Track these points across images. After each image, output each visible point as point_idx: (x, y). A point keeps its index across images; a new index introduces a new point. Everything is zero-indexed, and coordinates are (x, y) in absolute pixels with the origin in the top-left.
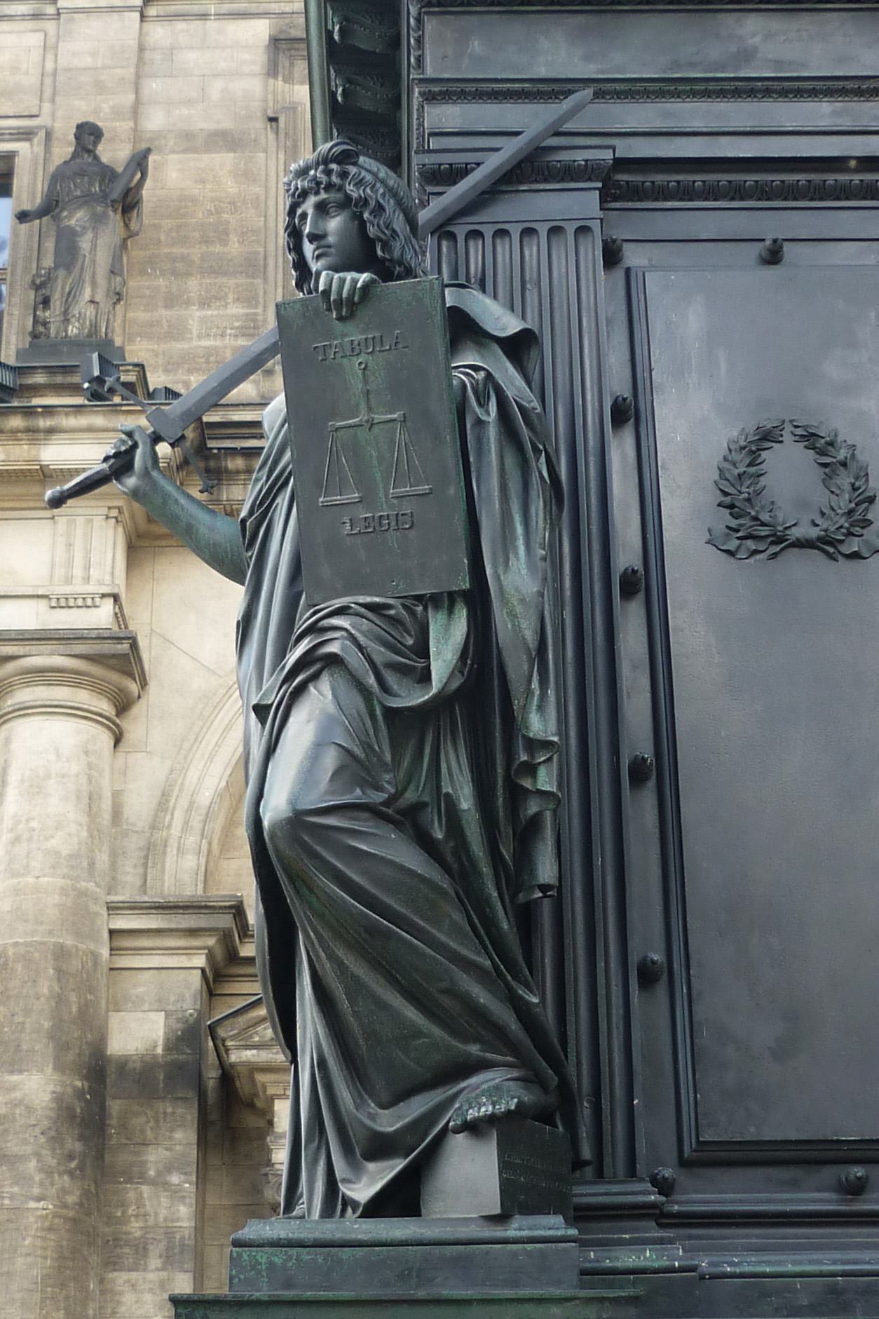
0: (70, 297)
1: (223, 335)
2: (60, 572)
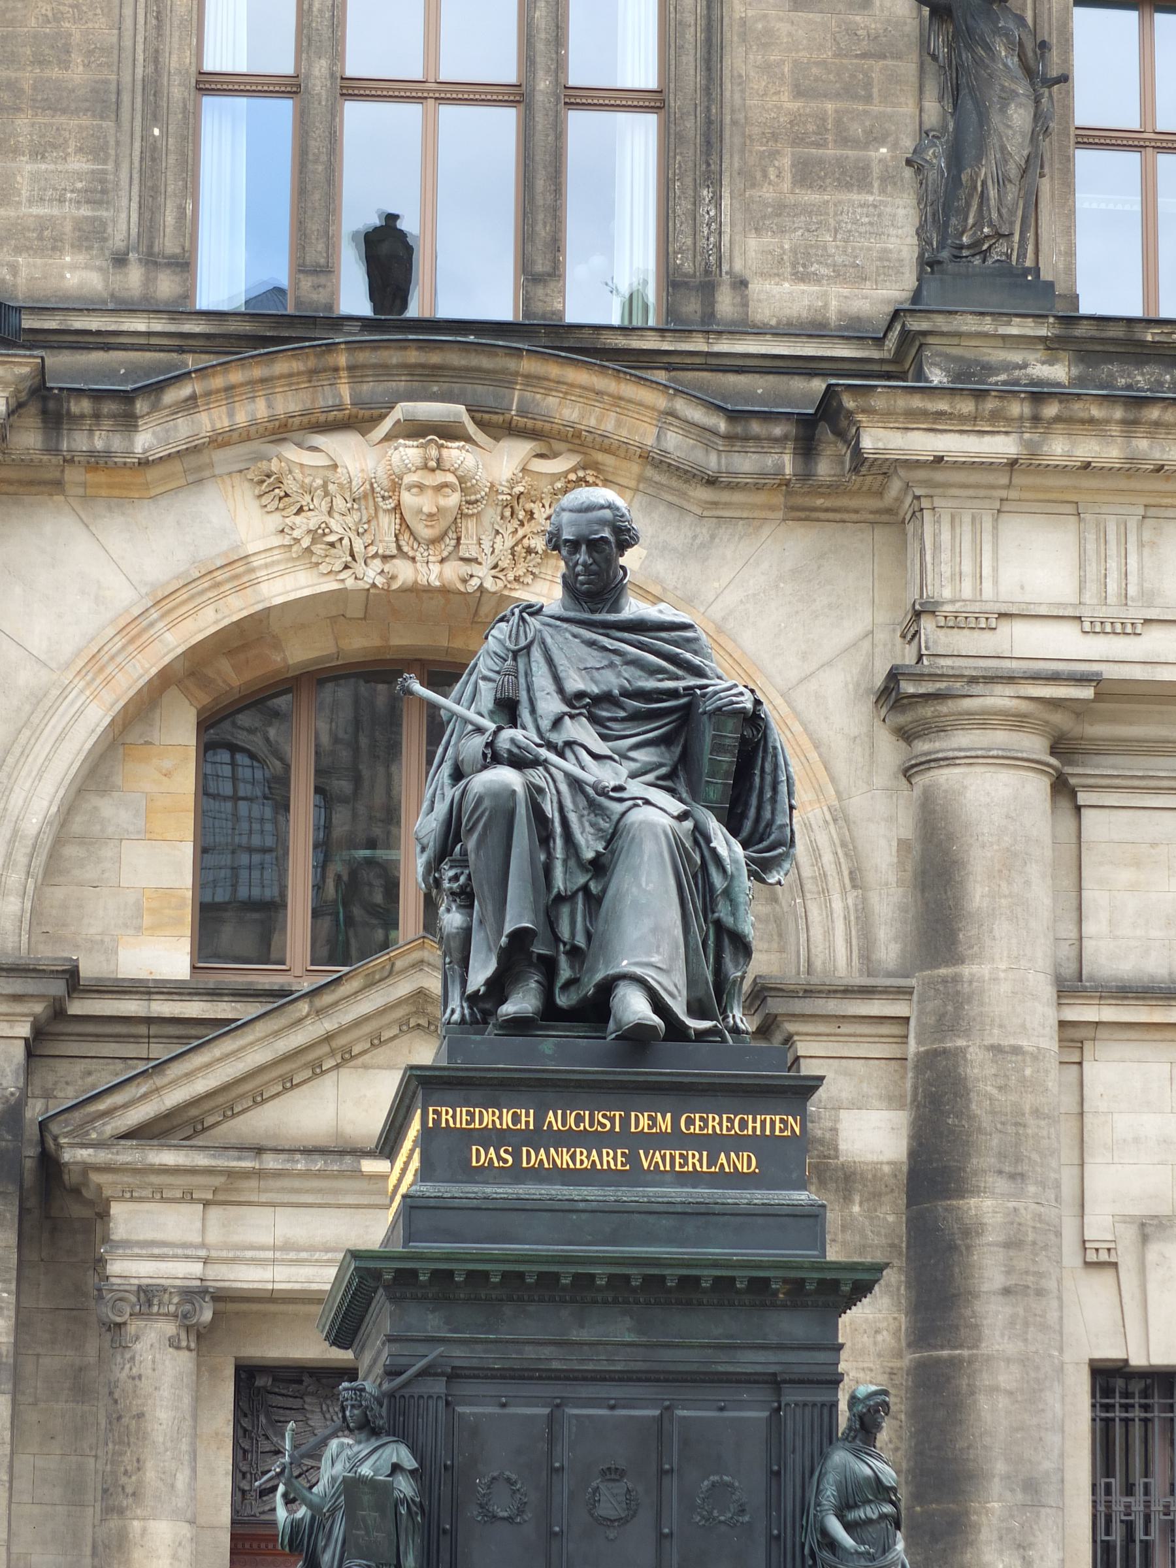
1: (61, 200)
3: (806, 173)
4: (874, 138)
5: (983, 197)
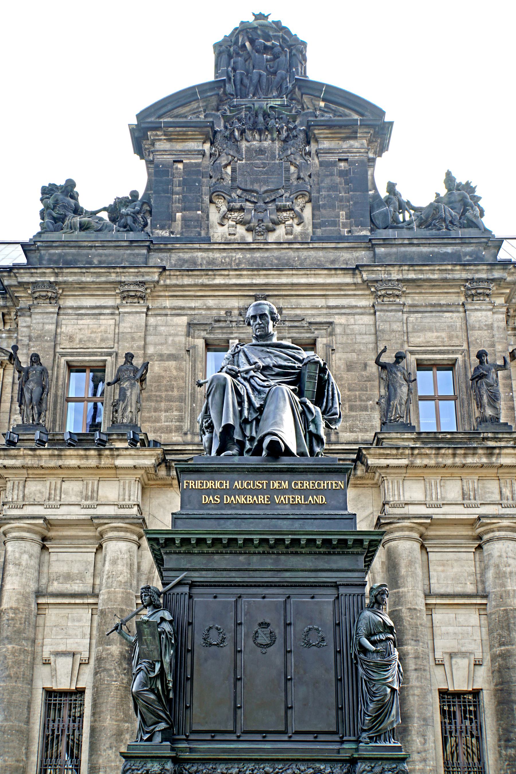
0: (125, 410)
2: (121, 497)
3: (352, 408)
4: (368, 399)
5: (396, 408)
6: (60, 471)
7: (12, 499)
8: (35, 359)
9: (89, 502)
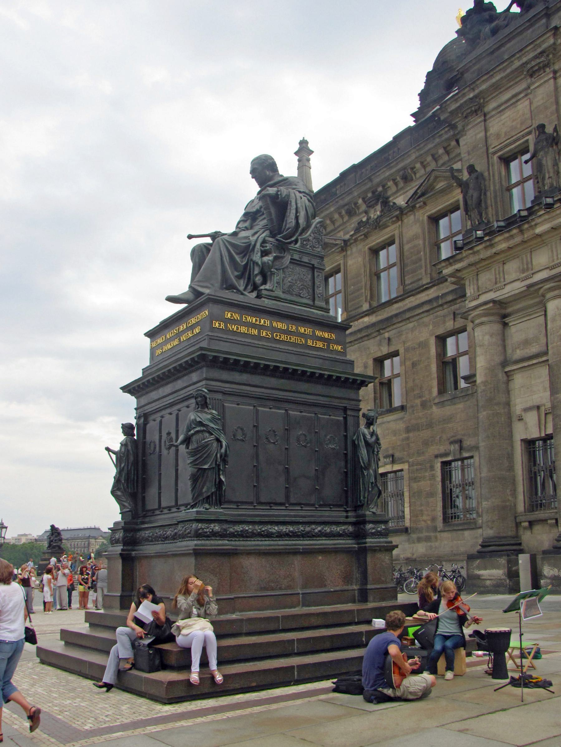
0: (543, 179)
6: (498, 257)
7: (470, 293)
8: (471, 169)
9: (524, 275)
